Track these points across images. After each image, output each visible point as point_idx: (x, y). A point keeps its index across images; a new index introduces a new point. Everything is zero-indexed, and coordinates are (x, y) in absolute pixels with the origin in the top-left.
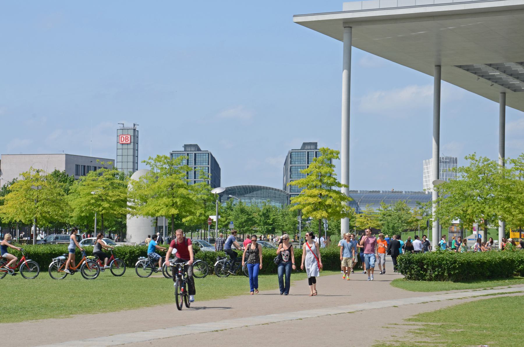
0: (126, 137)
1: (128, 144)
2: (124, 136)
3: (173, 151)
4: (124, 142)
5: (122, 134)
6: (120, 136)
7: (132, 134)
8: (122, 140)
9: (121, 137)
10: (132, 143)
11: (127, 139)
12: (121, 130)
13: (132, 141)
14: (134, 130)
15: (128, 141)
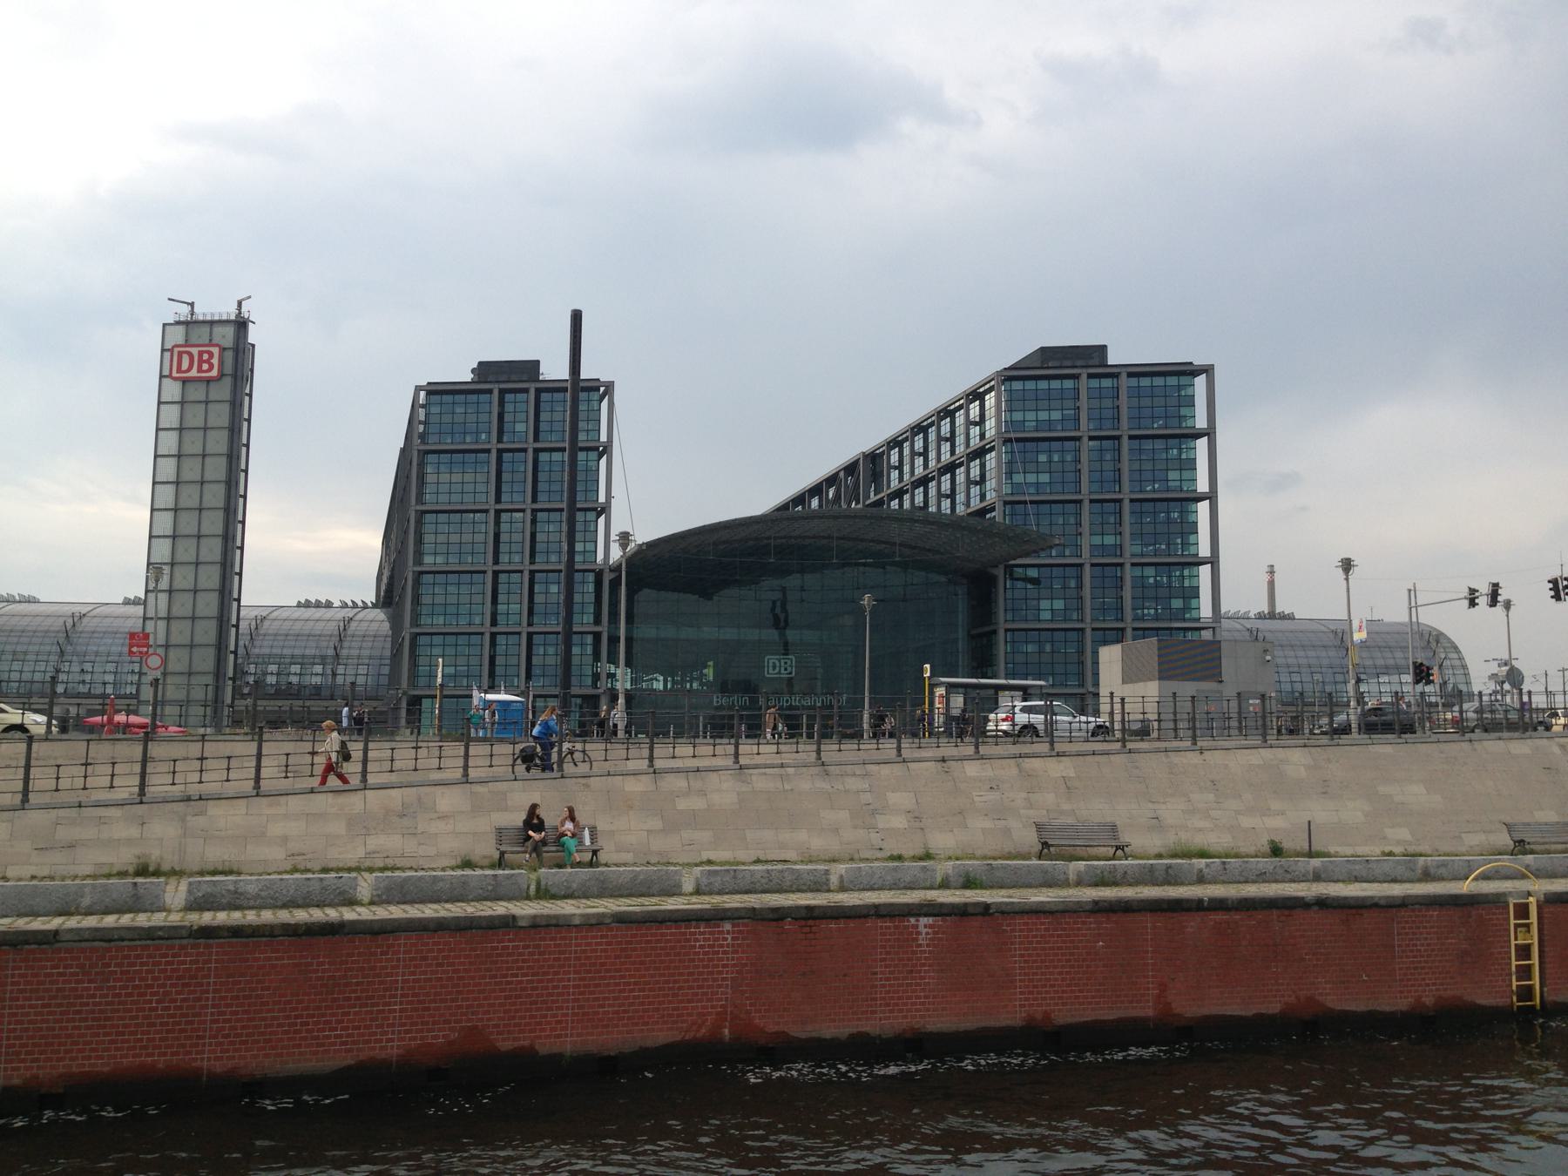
0: (201, 354)
1: (208, 381)
2: (195, 351)
3: (429, 383)
4: (194, 373)
5: (181, 342)
6: (176, 350)
7: (228, 341)
8: (185, 366)
9: (180, 354)
10: (227, 382)
11: (205, 362)
12: (181, 329)
13: (228, 369)
14: (241, 325)
15: (211, 367)
